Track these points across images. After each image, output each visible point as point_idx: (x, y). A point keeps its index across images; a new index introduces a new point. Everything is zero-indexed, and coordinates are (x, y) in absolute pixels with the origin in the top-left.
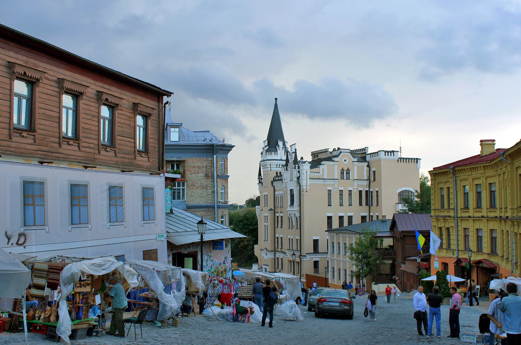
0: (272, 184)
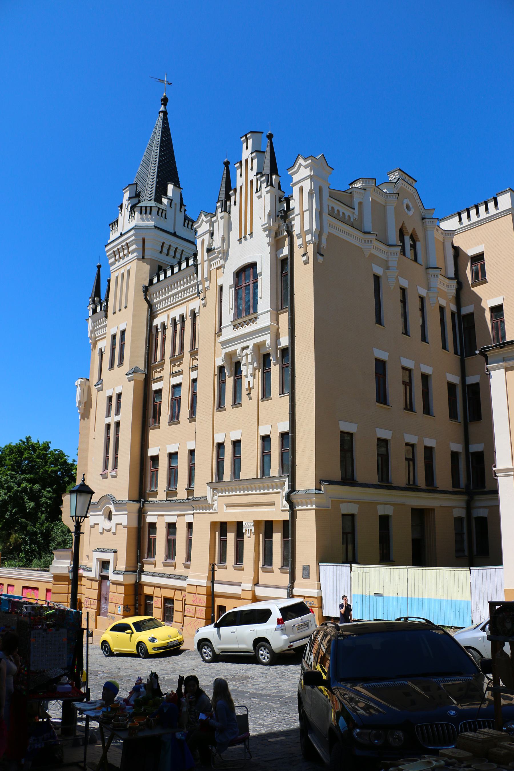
0: (146, 295)
